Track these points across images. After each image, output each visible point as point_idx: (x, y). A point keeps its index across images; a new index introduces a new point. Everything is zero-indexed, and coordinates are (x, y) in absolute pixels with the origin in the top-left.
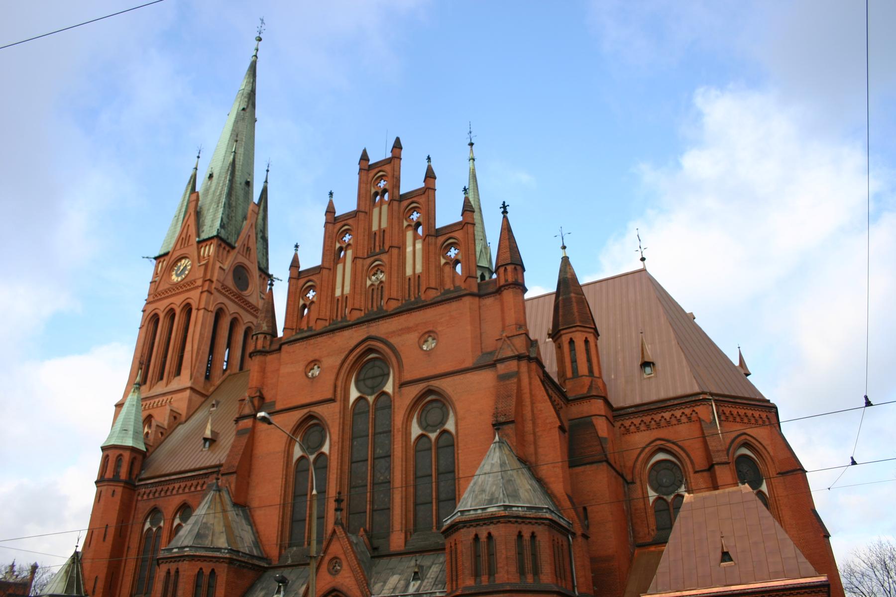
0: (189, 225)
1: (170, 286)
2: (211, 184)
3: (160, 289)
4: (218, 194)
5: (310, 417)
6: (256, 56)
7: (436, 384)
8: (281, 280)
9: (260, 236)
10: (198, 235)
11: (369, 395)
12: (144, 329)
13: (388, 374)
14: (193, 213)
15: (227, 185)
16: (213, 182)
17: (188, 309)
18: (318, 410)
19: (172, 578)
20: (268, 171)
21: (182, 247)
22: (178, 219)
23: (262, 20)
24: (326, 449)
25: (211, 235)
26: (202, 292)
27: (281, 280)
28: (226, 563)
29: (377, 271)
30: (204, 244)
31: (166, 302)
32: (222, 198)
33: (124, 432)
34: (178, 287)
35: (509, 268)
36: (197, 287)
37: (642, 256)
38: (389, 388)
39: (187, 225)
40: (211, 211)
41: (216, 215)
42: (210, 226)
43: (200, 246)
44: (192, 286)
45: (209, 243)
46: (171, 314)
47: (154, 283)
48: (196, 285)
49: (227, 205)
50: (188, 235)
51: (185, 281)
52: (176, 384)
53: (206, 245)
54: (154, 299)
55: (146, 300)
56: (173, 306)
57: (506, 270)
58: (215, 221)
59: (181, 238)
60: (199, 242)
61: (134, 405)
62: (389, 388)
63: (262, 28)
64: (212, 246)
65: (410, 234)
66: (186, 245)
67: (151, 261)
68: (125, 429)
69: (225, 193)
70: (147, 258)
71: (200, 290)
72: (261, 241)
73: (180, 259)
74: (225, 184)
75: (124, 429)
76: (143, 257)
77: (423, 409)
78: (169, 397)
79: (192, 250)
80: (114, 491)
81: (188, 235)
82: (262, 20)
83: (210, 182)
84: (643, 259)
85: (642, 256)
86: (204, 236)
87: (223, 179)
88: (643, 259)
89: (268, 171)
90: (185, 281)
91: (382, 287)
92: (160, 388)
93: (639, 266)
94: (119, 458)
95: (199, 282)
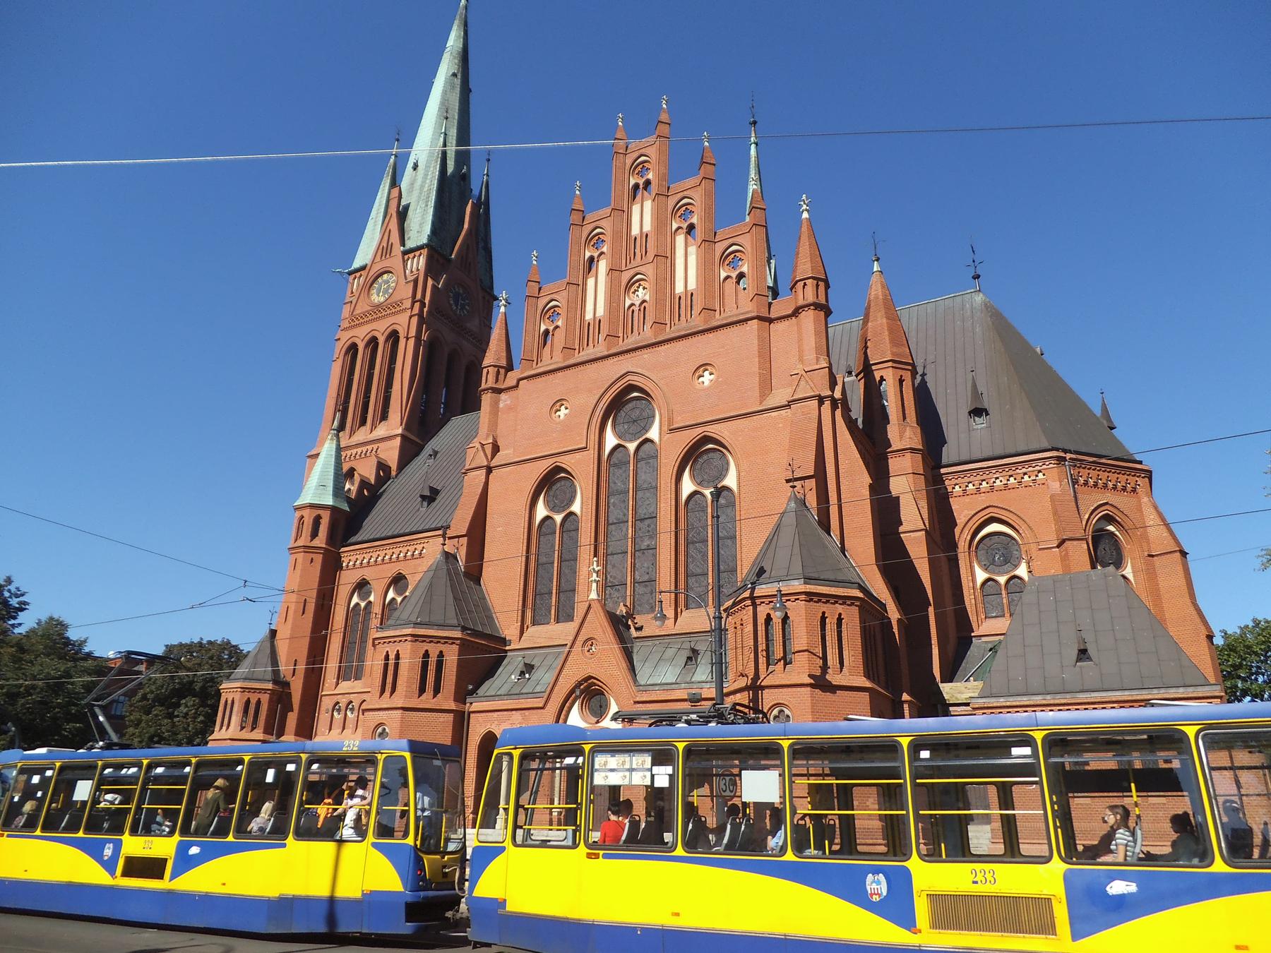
0: (390, 230)
1: (370, 308)
2: (416, 176)
3: (357, 312)
4: (426, 189)
5: (558, 469)
7: (712, 430)
9: (481, 245)
10: (403, 244)
14: (394, 215)
17: (394, 337)
18: (566, 462)
19: (392, 662)
21: (383, 257)
22: (376, 222)
24: (576, 507)
25: (420, 243)
26: (411, 317)
28: (457, 645)
29: (638, 287)
30: (411, 255)
31: (367, 328)
32: (431, 195)
34: (384, 307)
35: (809, 282)
38: (654, 433)
39: (388, 230)
40: (418, 211)
41: (425, 216)
42: (418, 232)
43: (406, 257)
45: (417, 253)
46: (373, 342)
50: (390, 243)
51: (388, 301)
52: (381, 431)
53: (414, 257)
56: (376, 334)
58: (424, 225)
59: (381, 247)
60: (405, 253)
61: (332, 455)
62: (654, 433)
64: (421, 257)
65: (680, 239)
66: (388, 256)
69: (435, 188)
71: (408, 313)
72: (483, 252)
73: (381, 275)
74: (435, 177)
78: (375, 446)
79: (395, 261)
81: (390, 243)
86: (410, 244)
87: (432, 169)
90: (388, 301)
91: (645, 308)
92: (362, 435)
94: (317, 521)
95: (408, 304)
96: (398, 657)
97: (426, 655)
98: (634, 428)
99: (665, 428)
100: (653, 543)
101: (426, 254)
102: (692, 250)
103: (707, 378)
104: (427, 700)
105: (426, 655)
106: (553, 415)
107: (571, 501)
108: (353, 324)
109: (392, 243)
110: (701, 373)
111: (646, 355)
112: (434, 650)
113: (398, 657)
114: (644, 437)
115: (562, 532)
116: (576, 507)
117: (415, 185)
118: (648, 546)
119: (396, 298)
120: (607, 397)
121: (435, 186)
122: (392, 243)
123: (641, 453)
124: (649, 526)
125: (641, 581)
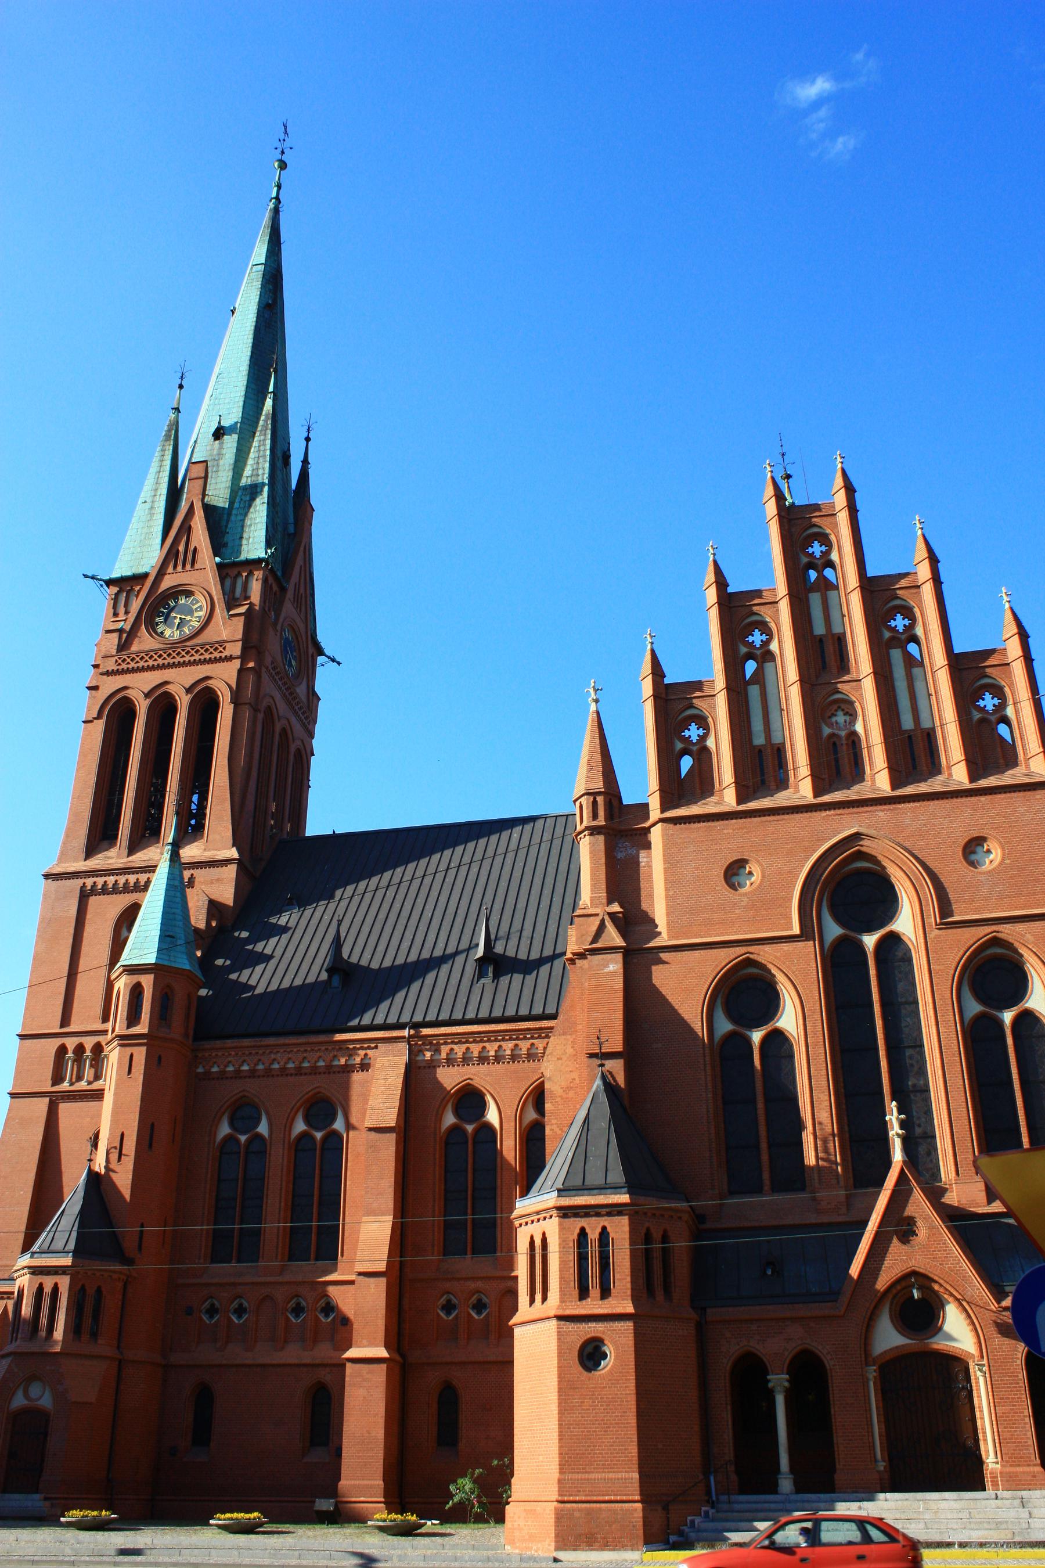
2: (221, 448)
6: (277, 198)
8: (339, 663)
12: (100, 725)
15: (268, 459)
16: (225, 446)
20: (308, 439)
22: (152, 508)
23: (285, 127)
27: (339, 663)
33: (169, 939)
36: (230, 658)
44: (216, 655)
47: (116, 635)
48: (227, 653)
49: (270, 498)
54: (120, 668)
55: (96, 666)
63: (287, 144)
66: (188, 567)
67: (102, 586)
68: (171, 934)
70: (93, 578)
75: (168, 934)
76: (85, 576)
80: (160, 1057)
82: (285, 127)
83: (217, 442)
89: (308, 439)
95: (236, 649)
96: (544, 1240)
97: (583, 1233)
101: (261, 576)
104: (594, 1305)
105: (583, 1233)
108: (124, 666)
109: (195, 549)
112: (593, 1227)
113: (544, 1240)
117: (221, 462)
119: (209, 635)
121: (267, 471)
122: (195, 549)
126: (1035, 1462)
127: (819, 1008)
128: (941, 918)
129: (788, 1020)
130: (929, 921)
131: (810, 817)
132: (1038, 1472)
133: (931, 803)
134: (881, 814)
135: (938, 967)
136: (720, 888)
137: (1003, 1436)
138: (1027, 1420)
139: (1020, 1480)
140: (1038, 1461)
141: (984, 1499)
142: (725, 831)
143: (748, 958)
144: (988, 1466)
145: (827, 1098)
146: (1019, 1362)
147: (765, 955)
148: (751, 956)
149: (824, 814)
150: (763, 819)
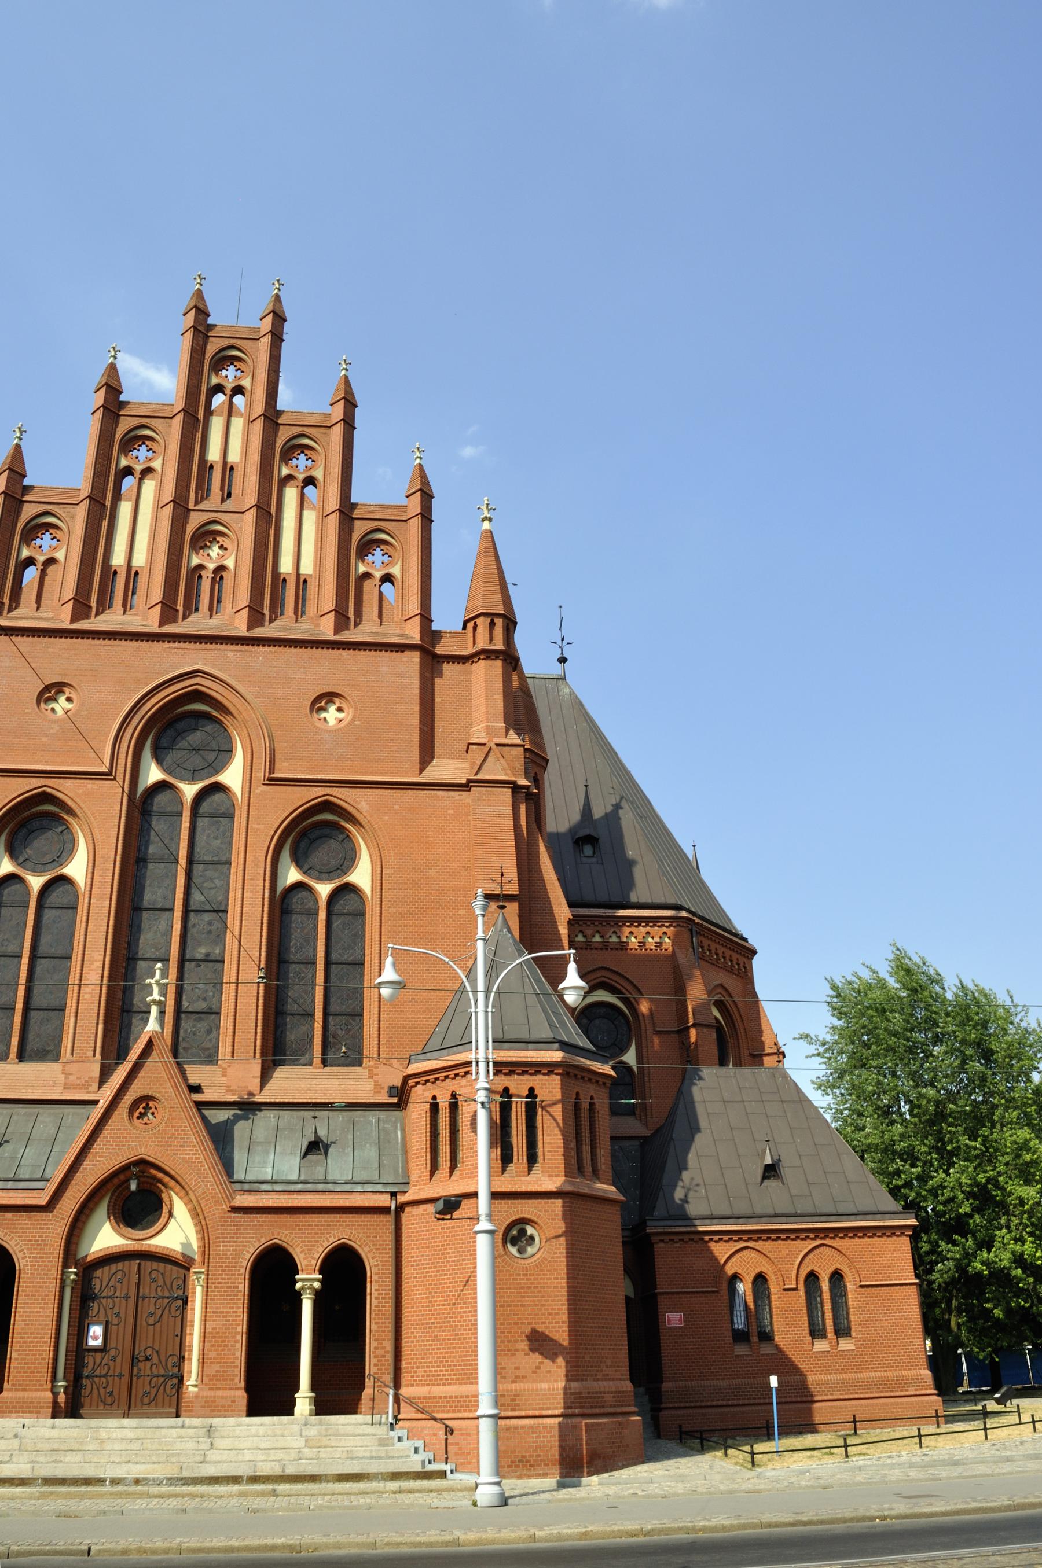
11: (183, 779)
13: (230, 752)
37: (562, 653)
57: (492, 624)
77: (303, 834)
84: (563, 660)
85: (562, 653)
88: (563, 660)
93: (556, 669)
98: (196, 761)
99: (260, 774)
100: (217, 951)
102: (310, 517)
103: (332, 715)
106: (42, 705)
107: (67, 851)
110: (323, 704)
111: (231, 653)
114: (212, 780)
115: (40, 907)
116: (77, 868)
118: (208, 955)
120: (154, 700)
123: (205, 807)
124: (210, 923)
125: (190, 1009)
126: (239, 1386)
127: (113, 856)
128: (270, 773)
129: (77, 868)
130: (258, 775)
131: (150, 647)
132: (239, 1397)
133: (288, 650)
134: (230, 654)
135: (255, 826)
136: (29, 711)
137: (208, 1354)
138: (239, 1337)
139: (217, 1406)
140: (243, 1384)
141: (168, 1428)
142: (50, 650)
143: (44, 793)
144: (187, 1389)
145: (102, 958)
146: (242, 1271)
147: (67, 790)
148: (49, 790)
149: (166, 645)
150: (96, 641)
